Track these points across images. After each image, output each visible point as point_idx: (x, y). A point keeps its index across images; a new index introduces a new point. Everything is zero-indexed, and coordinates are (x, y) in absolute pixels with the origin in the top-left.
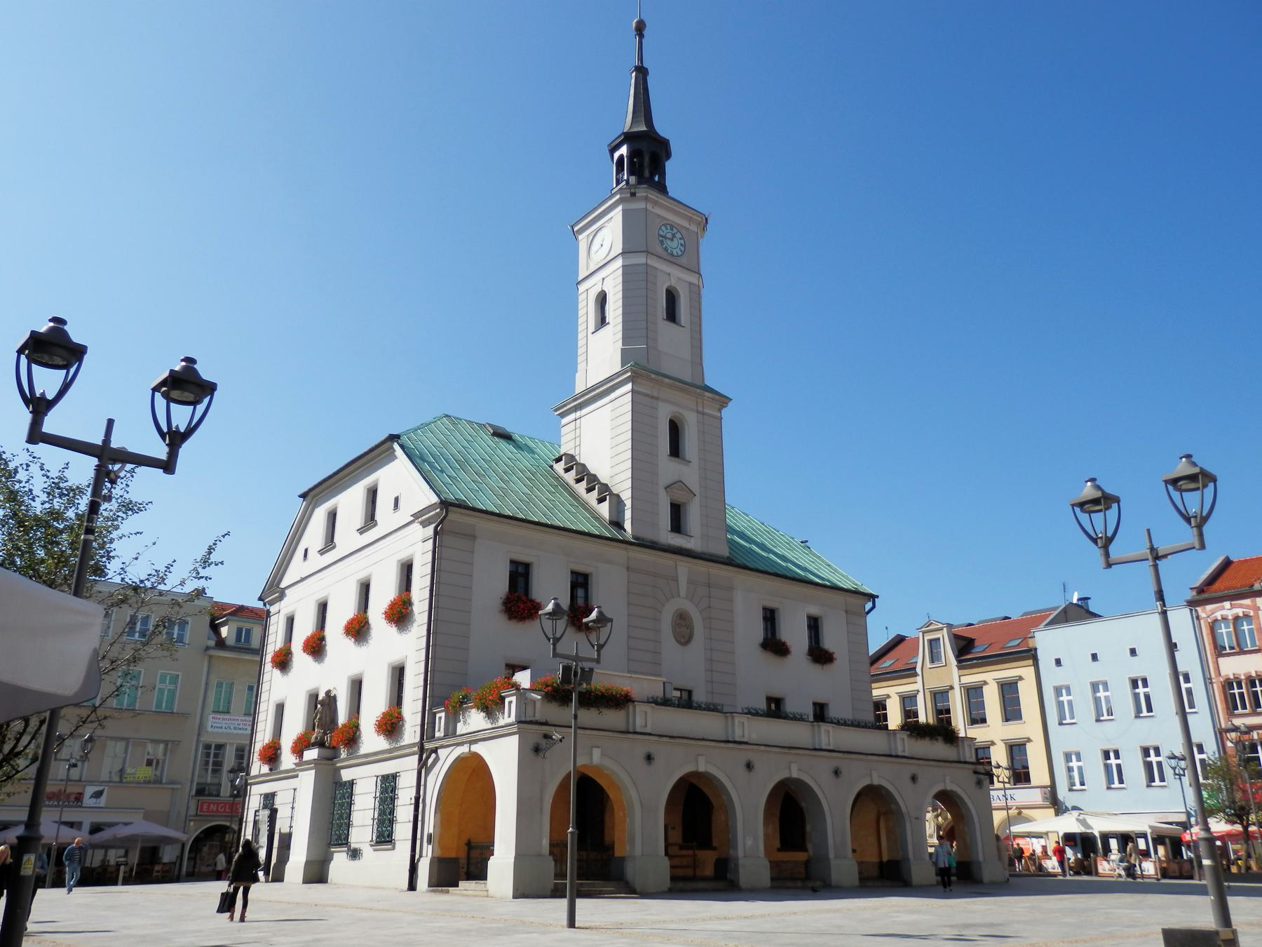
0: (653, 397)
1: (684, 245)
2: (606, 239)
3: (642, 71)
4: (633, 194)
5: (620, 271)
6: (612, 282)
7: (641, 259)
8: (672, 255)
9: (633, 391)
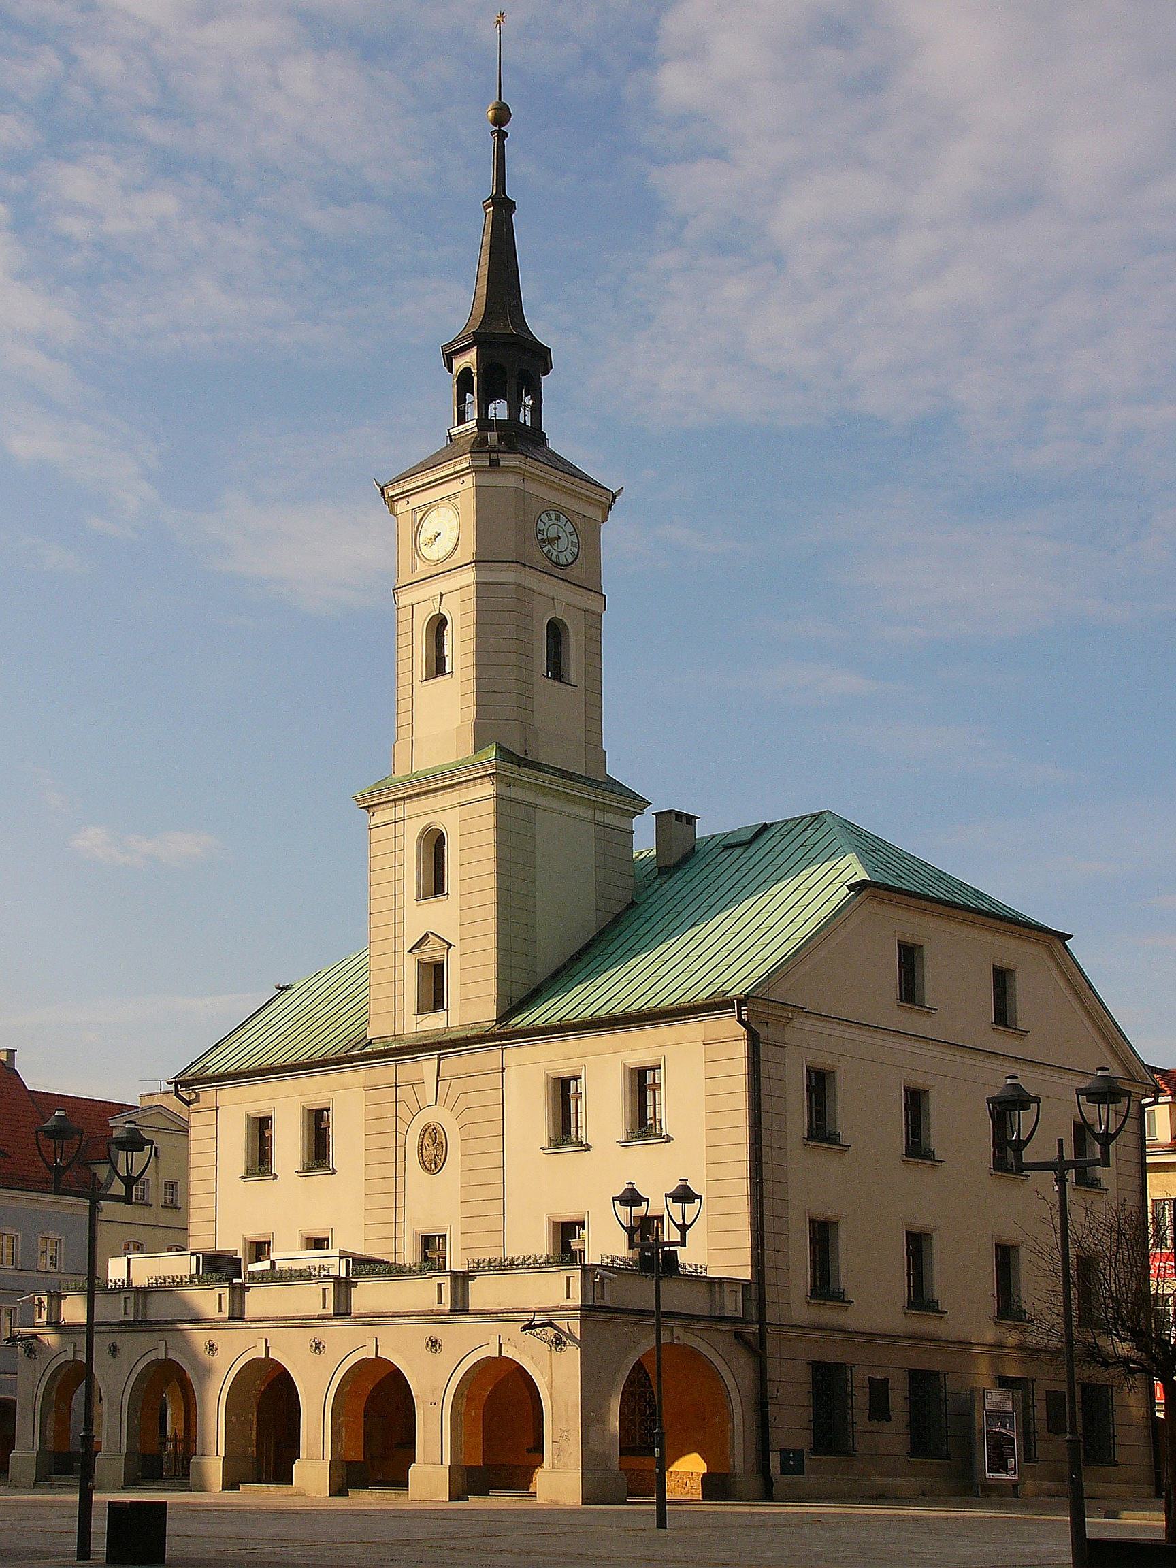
0: (527, 804)
1: (577, 545)
2: (447, 522)
3: (502, 206)
4: (494, 463)
5: (471, 591)
6: (457, 597)
7: (508, 575)
8: (557, 564)
9: (498, 797)
